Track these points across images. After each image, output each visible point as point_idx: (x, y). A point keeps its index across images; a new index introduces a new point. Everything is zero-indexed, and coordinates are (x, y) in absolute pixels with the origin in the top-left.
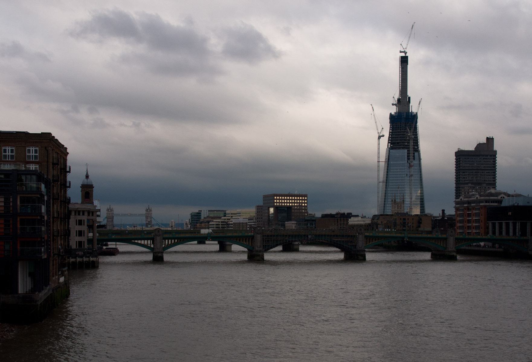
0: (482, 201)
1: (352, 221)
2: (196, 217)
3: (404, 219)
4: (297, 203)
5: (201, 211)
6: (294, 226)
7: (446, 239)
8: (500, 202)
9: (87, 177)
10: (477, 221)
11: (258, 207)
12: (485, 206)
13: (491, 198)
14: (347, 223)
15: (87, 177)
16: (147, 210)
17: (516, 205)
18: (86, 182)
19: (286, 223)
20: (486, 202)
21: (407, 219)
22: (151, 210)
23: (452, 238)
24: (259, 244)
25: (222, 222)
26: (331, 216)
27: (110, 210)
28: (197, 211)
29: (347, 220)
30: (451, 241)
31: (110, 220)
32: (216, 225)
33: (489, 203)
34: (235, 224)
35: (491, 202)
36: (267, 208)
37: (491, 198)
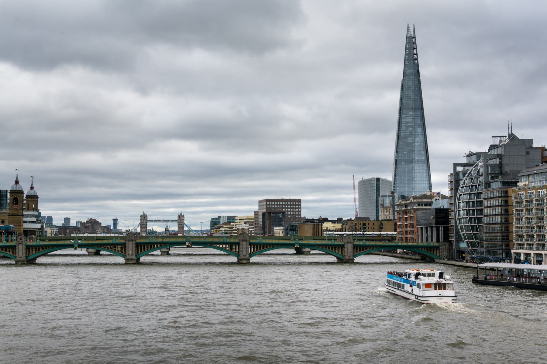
0: (412, 204)
1: (325, 225)
2: (215, 223)
3: (364, 224)
4: (291, 208)
5: (220, 217)
6: (281, 231)
7: (342, 247)
8: (430, 204)
9: (17, 182)
10: (412, 226)
11: (256, 213)
12: (417, 209)
13: (424, 200)
14: (322, 228)
15: (17, 182)
16: (179, 217)
17: (442, 208)
18: (17, 188)
19: (275, 228)
20: (419, 205)
21: (367, 224)
22: (183, 216)
23: (349, 245)
24: (130, 253)
25: (230, 228)
26: (312, 221)
27: (144, 217)
28: (217, 217)
29: (322, 225)
30: (349, 248)
31: (144, 226)
32: (225, 230)
33: (422, 205)
34: (238, 229)
35: (425, 205)
36: (261, 214)
37: (424, 200)
